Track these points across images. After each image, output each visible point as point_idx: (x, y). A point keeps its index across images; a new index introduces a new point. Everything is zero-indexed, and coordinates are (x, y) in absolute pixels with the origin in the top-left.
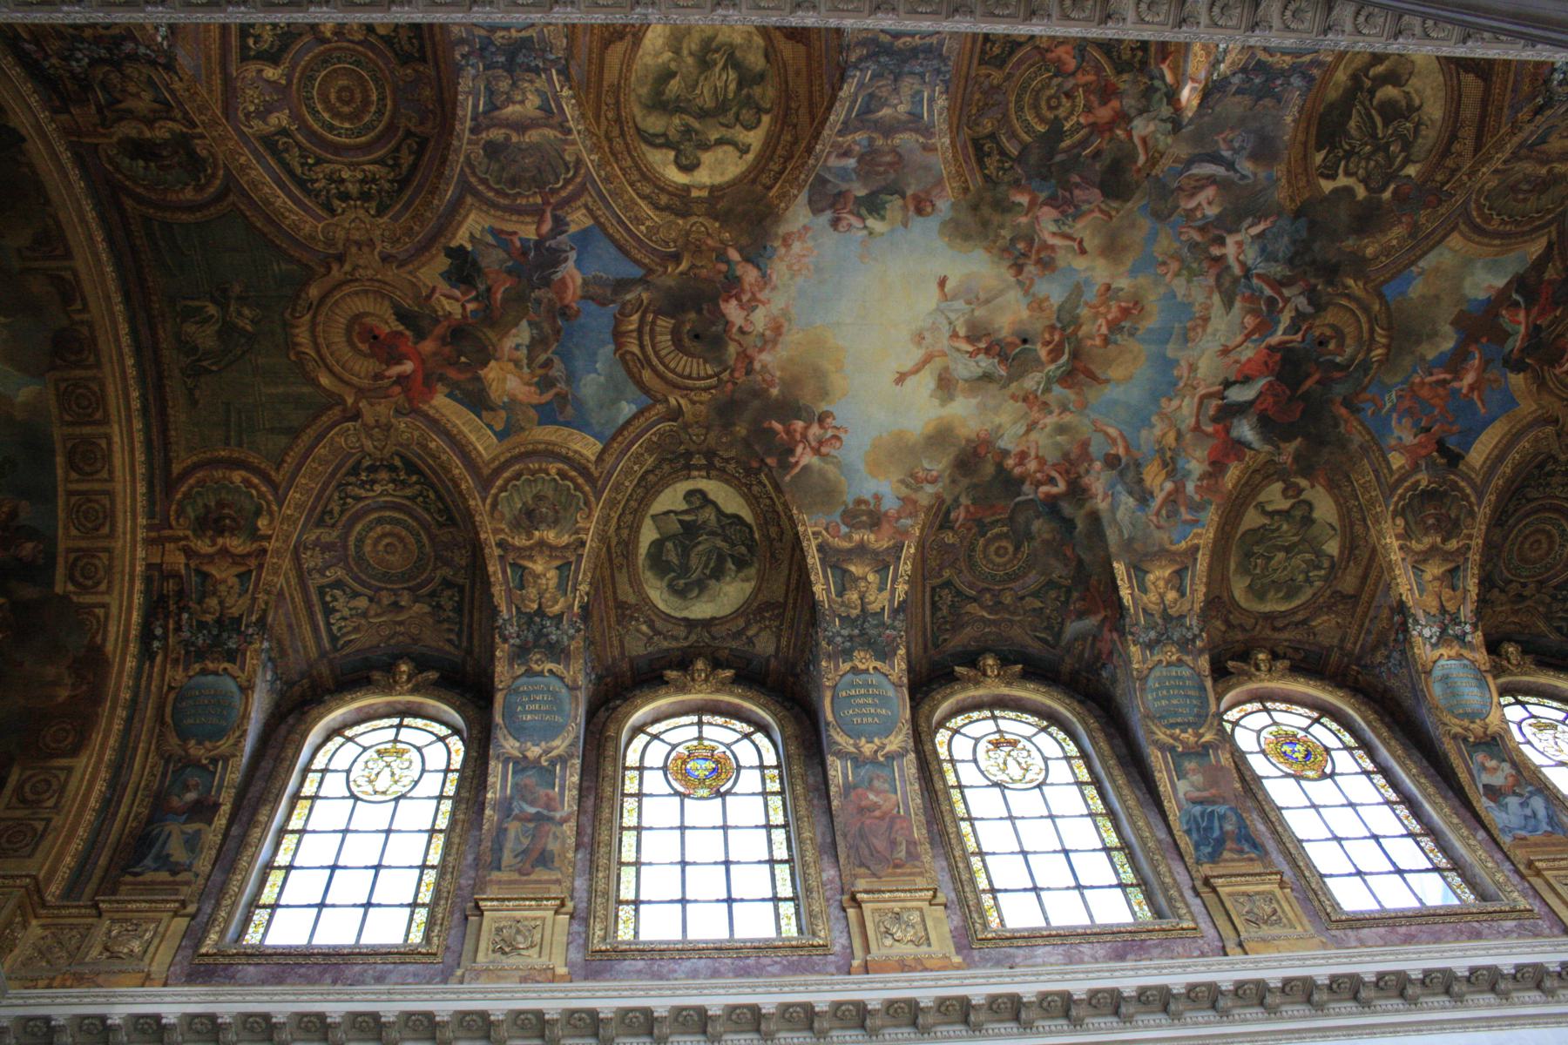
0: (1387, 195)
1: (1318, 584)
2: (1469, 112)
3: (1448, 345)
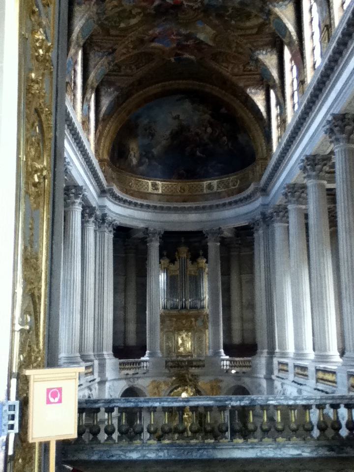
1: (110, 24)
2: (249, 32)
3: (183, 32)
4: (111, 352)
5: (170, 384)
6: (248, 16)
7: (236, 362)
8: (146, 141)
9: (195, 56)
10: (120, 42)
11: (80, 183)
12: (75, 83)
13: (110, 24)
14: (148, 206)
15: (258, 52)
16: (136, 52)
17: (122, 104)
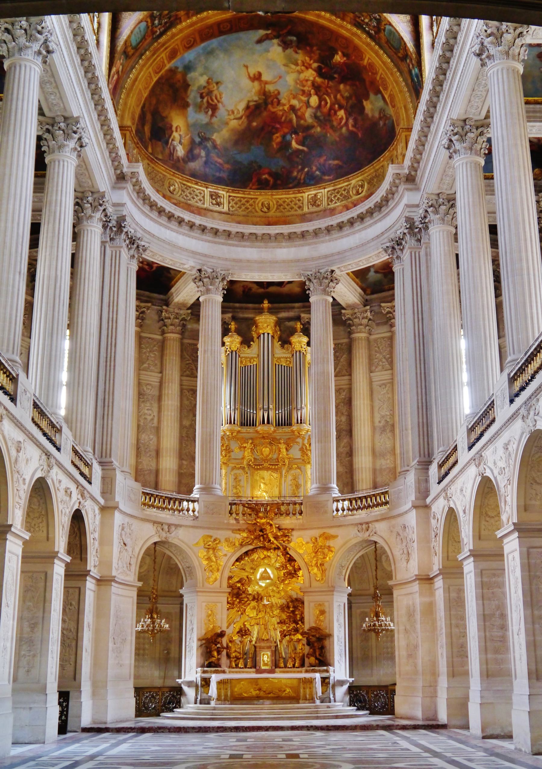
5: (237, 544)
8: (203, 118)
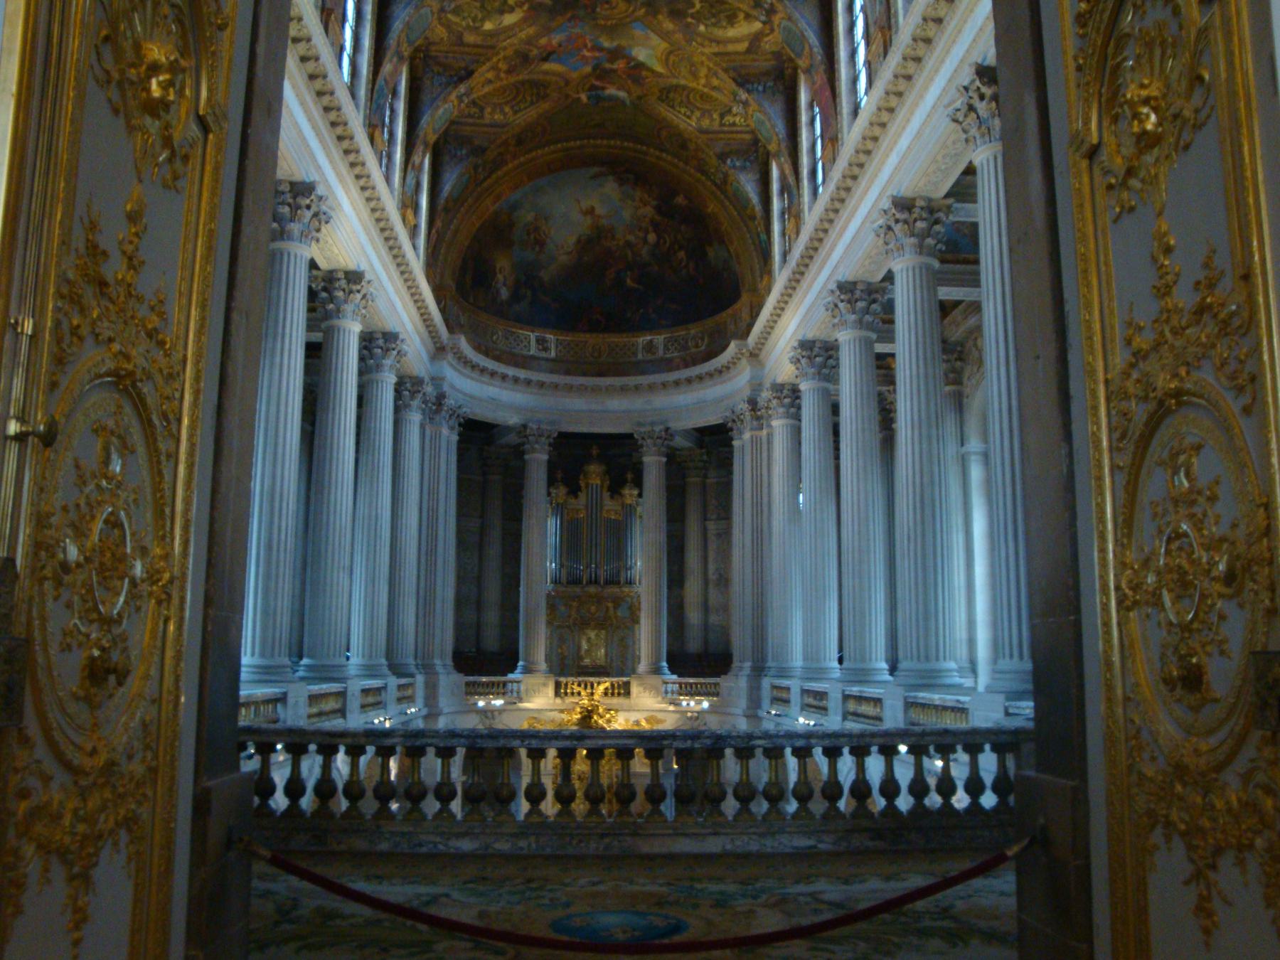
0: (689, 20)
2: (731, 48)
3: (606, 44)
4: (449, 662)
6: (732, 20)
7: (691, 685)
9: (629, 92)
10: (482, 59)
11: (391, 325)
12: (392, 134)
13: (464, 23)
14: (528, 382)
15: (750, 87)
16: (513, 79)
17: (485, 179)
